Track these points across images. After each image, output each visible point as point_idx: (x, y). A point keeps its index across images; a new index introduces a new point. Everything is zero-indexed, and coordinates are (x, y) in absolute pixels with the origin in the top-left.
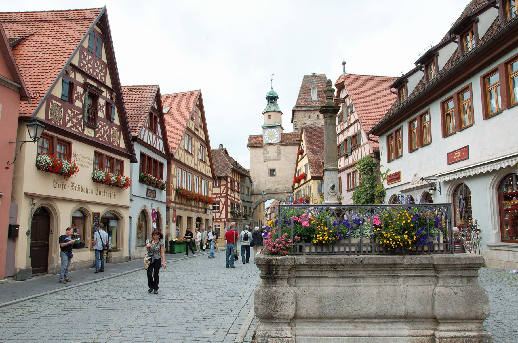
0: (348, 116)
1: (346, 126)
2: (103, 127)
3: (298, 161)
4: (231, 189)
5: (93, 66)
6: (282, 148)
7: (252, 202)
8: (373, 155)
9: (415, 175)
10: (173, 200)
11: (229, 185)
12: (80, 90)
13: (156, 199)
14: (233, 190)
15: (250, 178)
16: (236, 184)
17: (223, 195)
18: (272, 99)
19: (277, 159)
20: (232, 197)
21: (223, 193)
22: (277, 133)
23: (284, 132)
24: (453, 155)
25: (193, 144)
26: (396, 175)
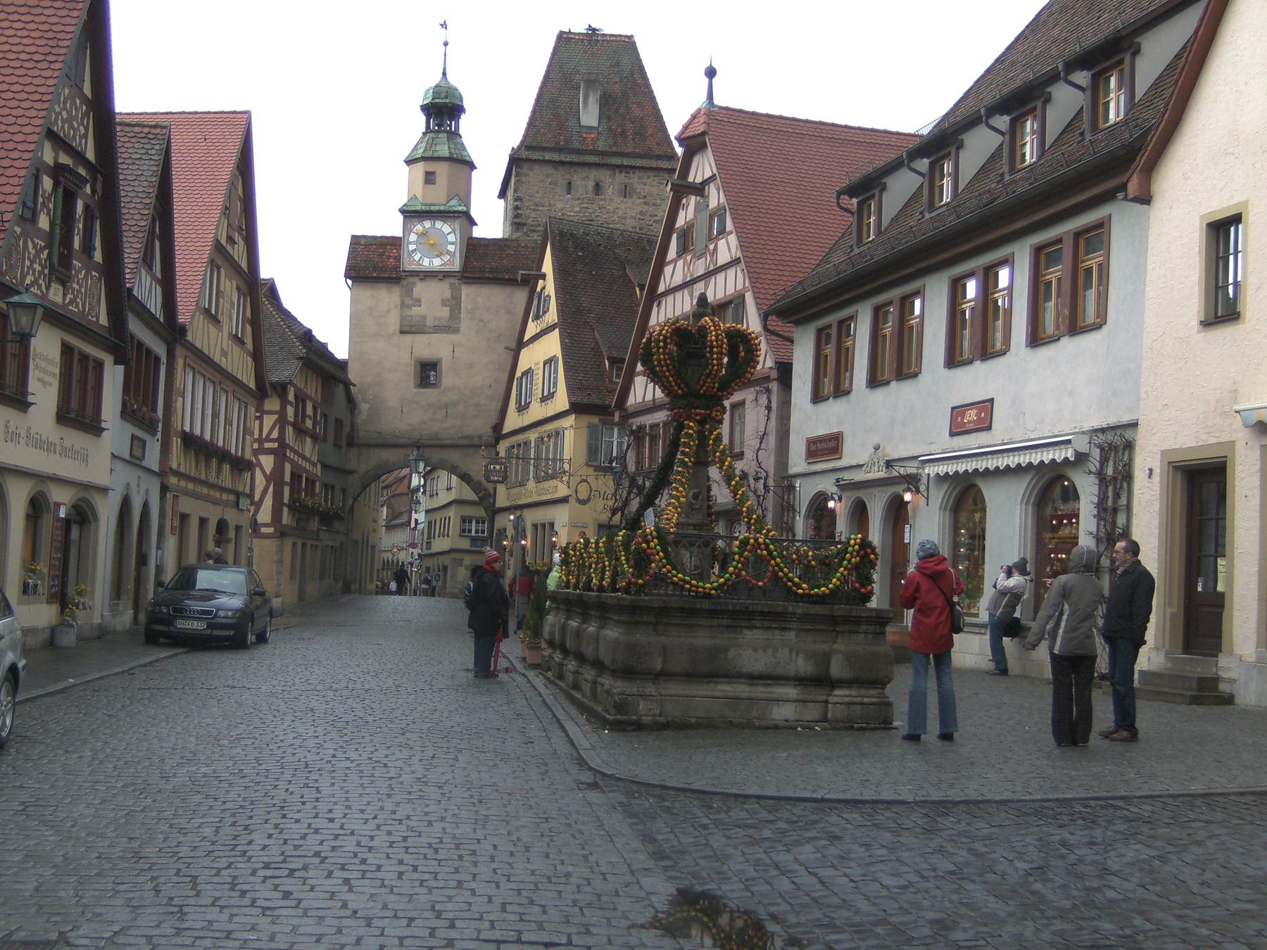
0: (710, 239)
1: (700, 268)
2: (79, 271)
3: (521, 344)
4: (294, 425)
5: (69, 113)
6: (467, 292)
7: (349, 472)
8: (774, 374)
9: (877, 448)
10: (175, 466)
11: (290, 411)
12: (47, 183)
13: (144, 463)
14: (300, 431)
15: (347, 384)
16: (309, 411)
17: (267, 445)
18: (443, 110)
19: (450, 327)
20: (296, 452)
21: (268, 440)
22: (451, 238)
23: (478, 232)
24: (963, 416)
25: (222, 288)
26: (830, 440)
